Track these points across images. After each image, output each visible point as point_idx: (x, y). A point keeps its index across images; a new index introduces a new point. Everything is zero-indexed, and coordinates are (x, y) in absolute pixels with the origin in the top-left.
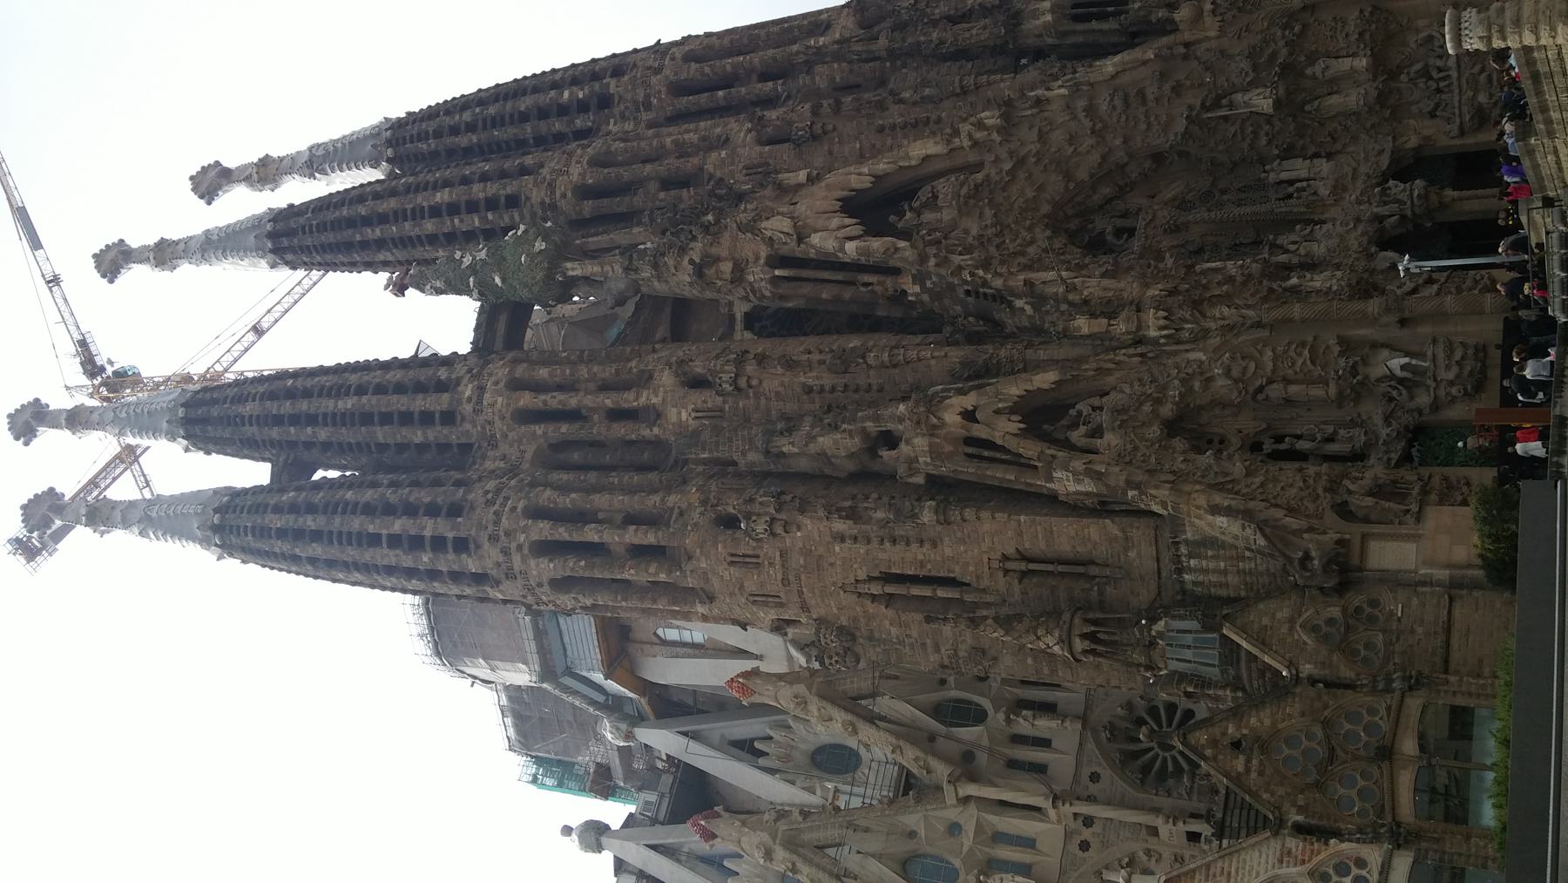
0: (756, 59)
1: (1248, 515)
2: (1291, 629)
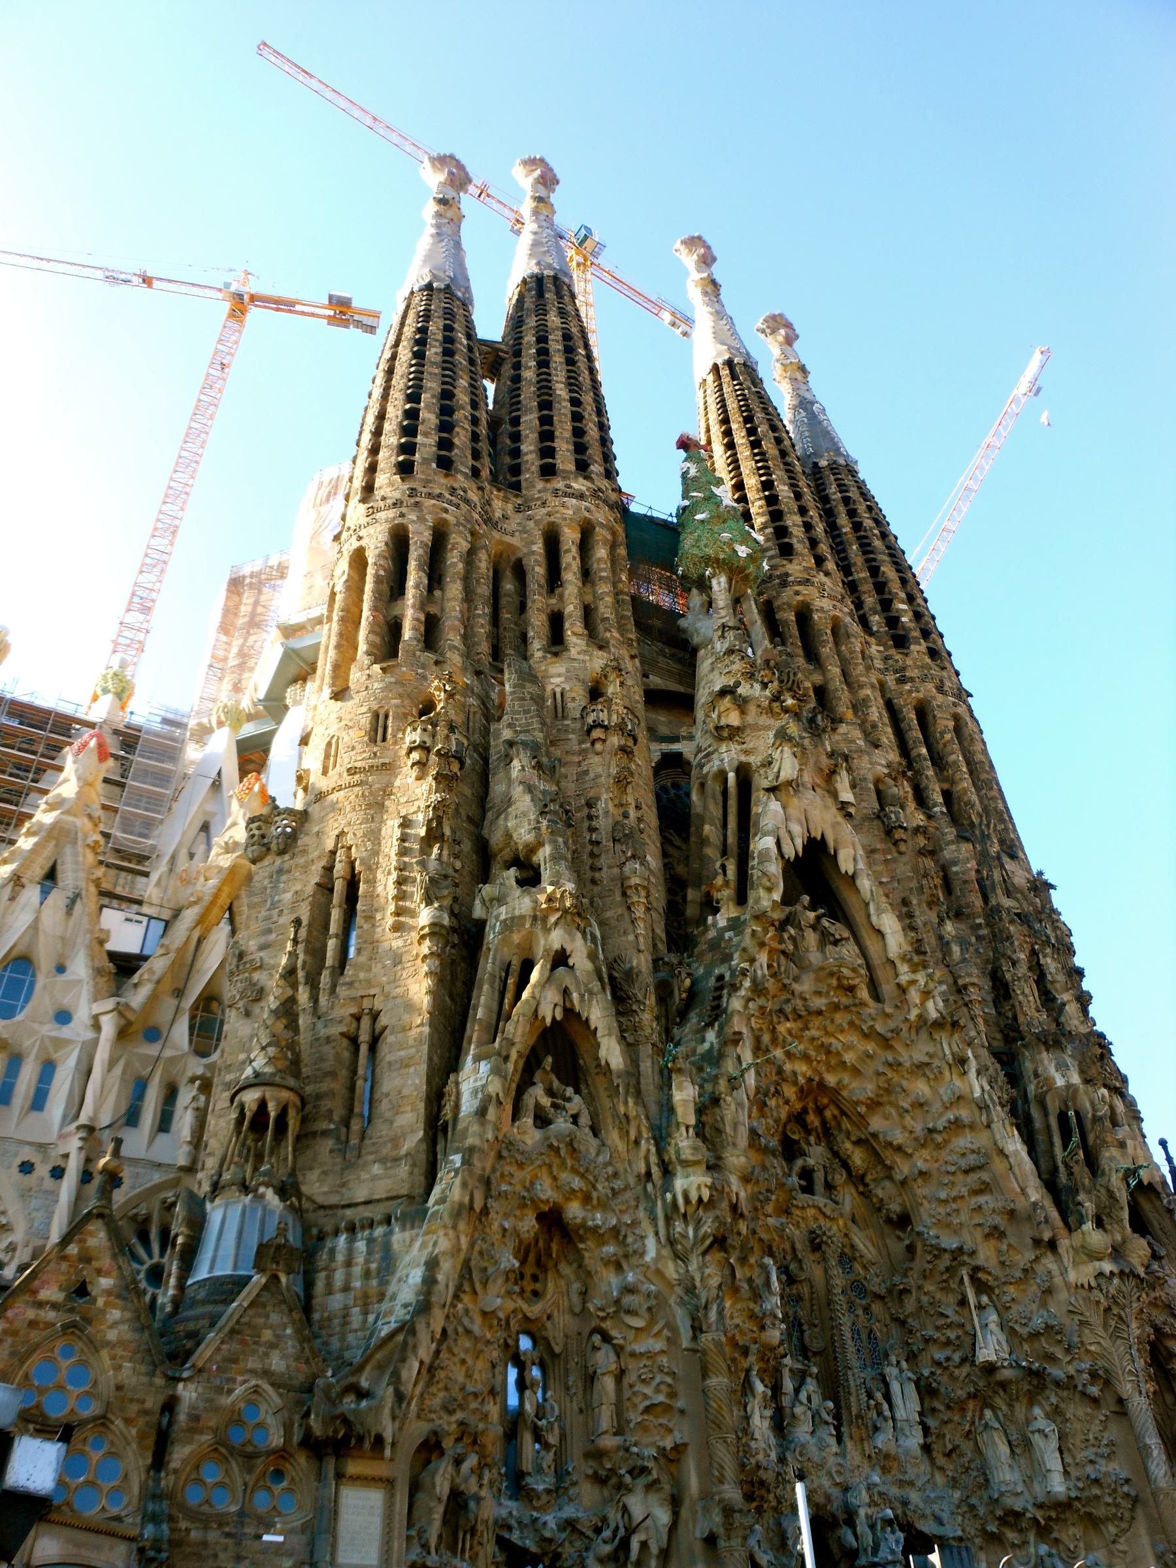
0: (966, 783)
1: (424, 1307)
2: (253, 1372)
